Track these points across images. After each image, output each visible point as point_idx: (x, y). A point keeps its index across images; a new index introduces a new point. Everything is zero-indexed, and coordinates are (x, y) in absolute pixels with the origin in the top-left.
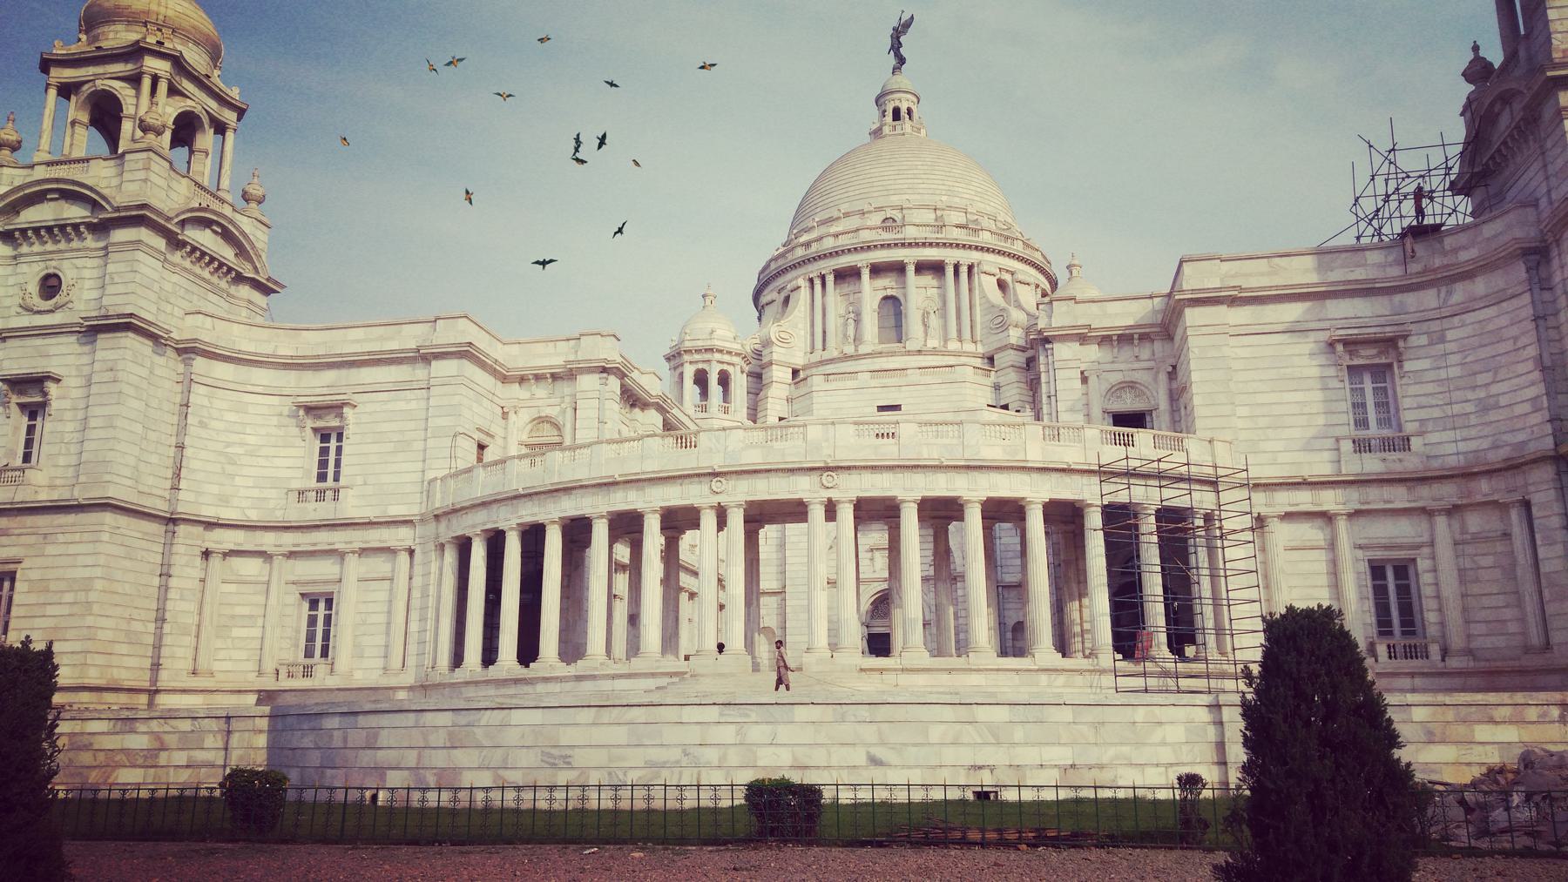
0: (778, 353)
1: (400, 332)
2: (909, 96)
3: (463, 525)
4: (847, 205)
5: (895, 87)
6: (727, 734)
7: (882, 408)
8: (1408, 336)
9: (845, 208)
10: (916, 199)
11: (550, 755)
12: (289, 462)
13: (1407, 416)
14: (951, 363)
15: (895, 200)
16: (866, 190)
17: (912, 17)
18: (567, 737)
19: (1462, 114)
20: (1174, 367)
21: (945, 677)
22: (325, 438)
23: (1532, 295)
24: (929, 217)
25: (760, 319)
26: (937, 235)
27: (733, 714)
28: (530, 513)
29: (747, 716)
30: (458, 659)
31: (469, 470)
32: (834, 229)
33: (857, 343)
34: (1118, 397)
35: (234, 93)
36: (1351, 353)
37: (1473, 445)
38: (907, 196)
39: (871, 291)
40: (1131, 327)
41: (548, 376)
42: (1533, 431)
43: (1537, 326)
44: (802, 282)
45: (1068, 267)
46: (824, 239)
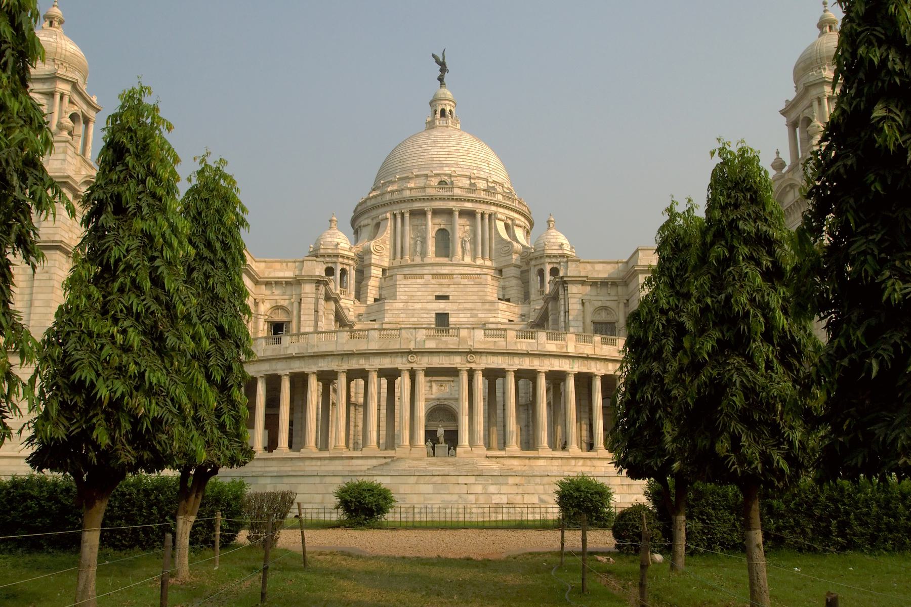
0: (375, 259)
2: (451, 103)
4: (416, 170)
6: (479, 489)
7: (439, 298)
9: (416, 172)
10: (459, 171)
14: (479, 272)
15: (447, 170)
16: (430, 162)
20: (628, 300)
21: (527, 462)
24: (466, 182)
27: (481, 480)
28: (297, 367)
32: (412, 185)
35: (95, 99)
40: (605, 278)
44: (388, 215)
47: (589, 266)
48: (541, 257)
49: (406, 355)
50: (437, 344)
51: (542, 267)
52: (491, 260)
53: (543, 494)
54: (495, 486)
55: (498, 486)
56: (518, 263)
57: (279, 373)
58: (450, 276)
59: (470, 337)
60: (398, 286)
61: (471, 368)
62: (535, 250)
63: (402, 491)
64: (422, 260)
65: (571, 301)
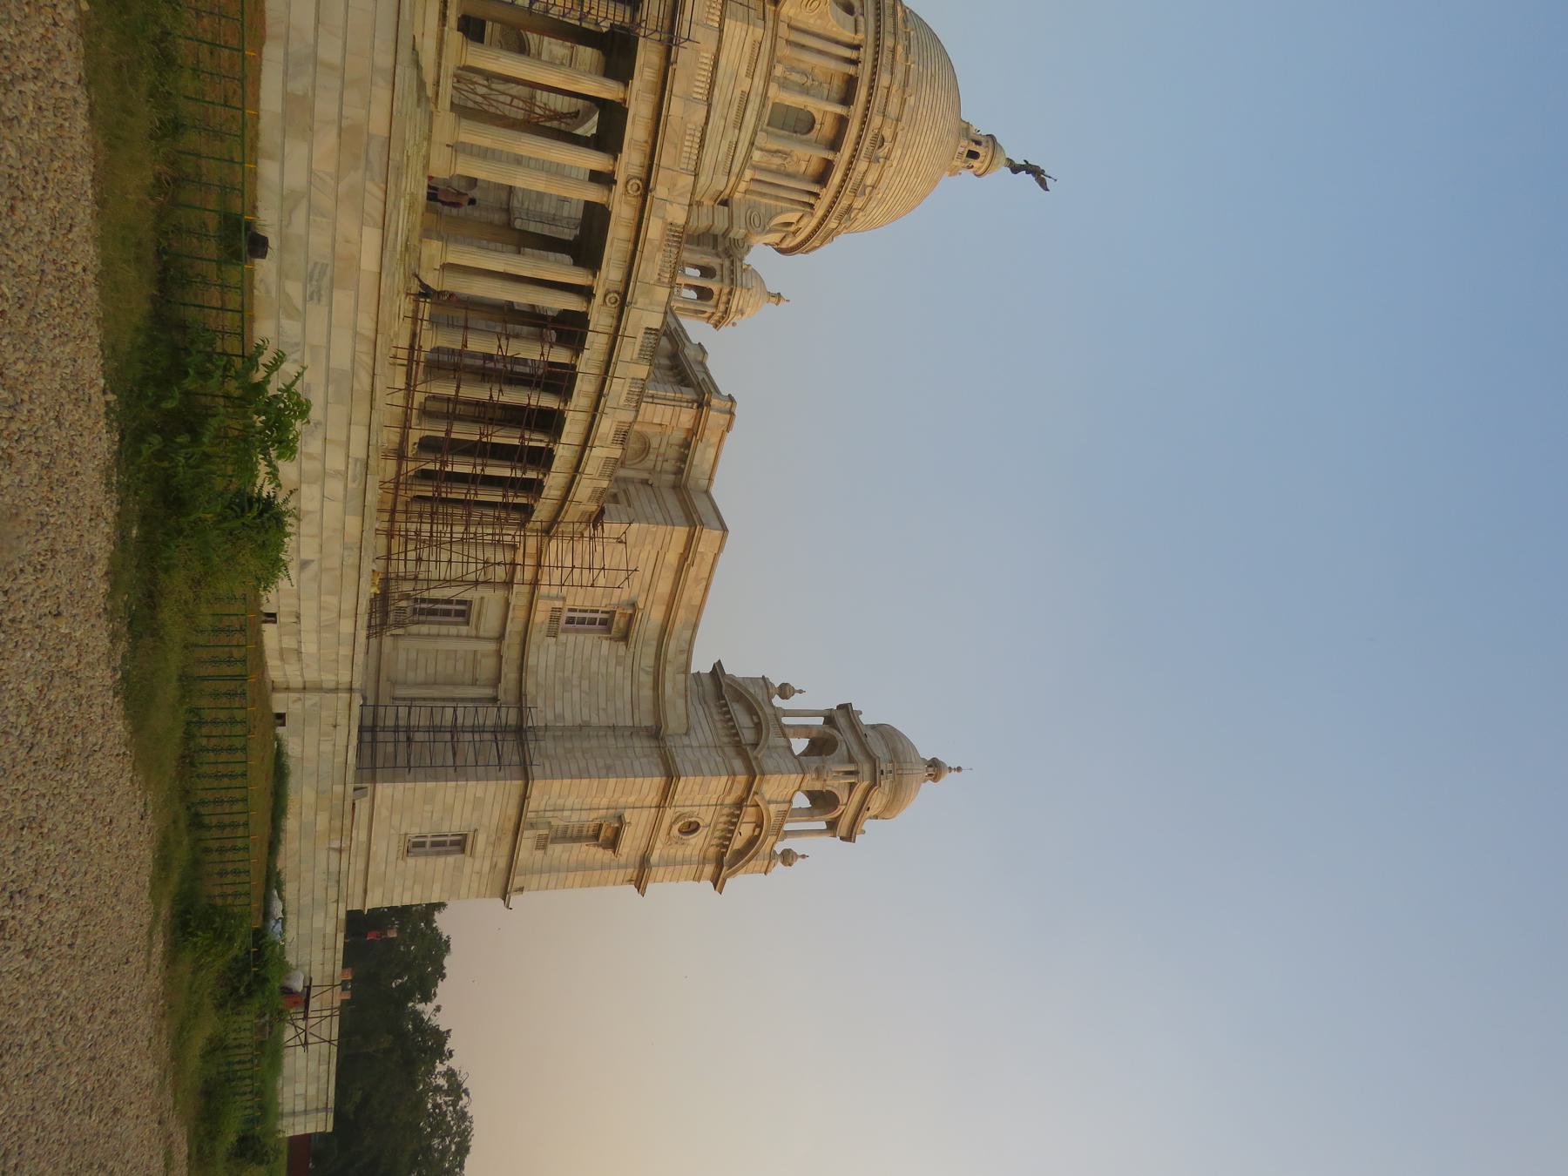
5: (995, 161)
6: (335, 461)
9: (911, 101)
10: (889, 172)
13: (572, 637)
15: (897, 153)
16: (916, 128)
17: (1047, 190)
18: (343, 300)
24: (869, 181)
26: (850, 186)
29: (354, 481)
36: (623, 615)
37: (541, 671)
38: (895, 164)
39: (825, 110)
40: (691, 463)
42: (542, 711)
43: (609, 727)
44: (861, 36)
45: (779, 294)
47: (715, 440)
48: (732, 279)
49: (644, 176)
51: (718, 277)
56: (731, 235)
58: (740, 125)
59: (651, 304)
60: (745, 26)
63: (339, 295)
65: (669, 410)
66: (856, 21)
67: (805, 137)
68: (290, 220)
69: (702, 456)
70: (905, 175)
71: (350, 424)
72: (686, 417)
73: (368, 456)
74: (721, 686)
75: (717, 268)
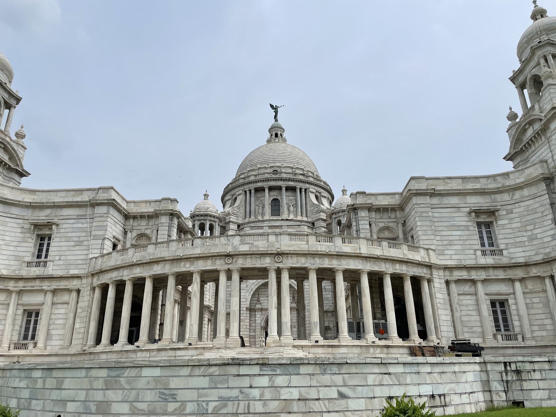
1: (82, 193)
3: (105, 279)
6: (264, 381)
8: (499, 210)
11: (164, 394)
12: (25, 249)
13: (500, 242)
18: (174, 383)
19: (507, 131)
20: (405, 221)
21: (330, 350)
22: (42, 239)
23: (549, 195)
24: (290, 171)
25: (224, 206)
27: (267, 371)
28: (138, 272)
29: (275, 371)
30: (98, 341)
31: (110, 254)
33: (263, 216)
34: (382, 233)
37: (527, 254)
38: (282, 163)
41: (146, 216)
42: (553, 248)
43: (552, 207)
46: (251, 177)
49: (224, 257)
50: (250, 248)
51: (340, 218)
52: (307, 216)
53: (342, 386)
54: (284, 376)
55: (287, 377)
56: (325, 218)
57: (124, 278)
61: (279, 268)
62: (335, 208)
63: (172, 386)
64: (262, 217)
65: (361, 222)
66: (238, 195)
67: (280, 200)
68: (142, 410)
69: (384, 202)
70: (285, 158)
71: (239, 375)
72: (363, 214)
73: (257, 364)
74: (516, 153)
75: (336, 220)
